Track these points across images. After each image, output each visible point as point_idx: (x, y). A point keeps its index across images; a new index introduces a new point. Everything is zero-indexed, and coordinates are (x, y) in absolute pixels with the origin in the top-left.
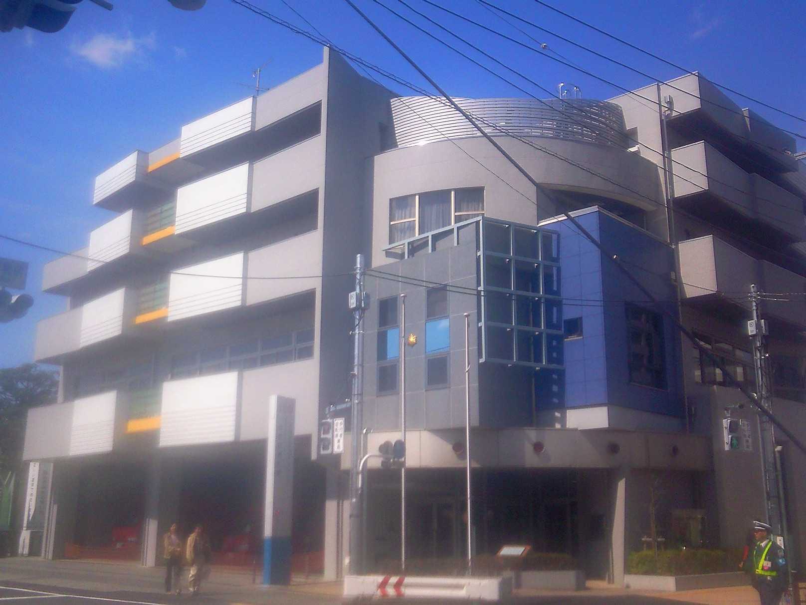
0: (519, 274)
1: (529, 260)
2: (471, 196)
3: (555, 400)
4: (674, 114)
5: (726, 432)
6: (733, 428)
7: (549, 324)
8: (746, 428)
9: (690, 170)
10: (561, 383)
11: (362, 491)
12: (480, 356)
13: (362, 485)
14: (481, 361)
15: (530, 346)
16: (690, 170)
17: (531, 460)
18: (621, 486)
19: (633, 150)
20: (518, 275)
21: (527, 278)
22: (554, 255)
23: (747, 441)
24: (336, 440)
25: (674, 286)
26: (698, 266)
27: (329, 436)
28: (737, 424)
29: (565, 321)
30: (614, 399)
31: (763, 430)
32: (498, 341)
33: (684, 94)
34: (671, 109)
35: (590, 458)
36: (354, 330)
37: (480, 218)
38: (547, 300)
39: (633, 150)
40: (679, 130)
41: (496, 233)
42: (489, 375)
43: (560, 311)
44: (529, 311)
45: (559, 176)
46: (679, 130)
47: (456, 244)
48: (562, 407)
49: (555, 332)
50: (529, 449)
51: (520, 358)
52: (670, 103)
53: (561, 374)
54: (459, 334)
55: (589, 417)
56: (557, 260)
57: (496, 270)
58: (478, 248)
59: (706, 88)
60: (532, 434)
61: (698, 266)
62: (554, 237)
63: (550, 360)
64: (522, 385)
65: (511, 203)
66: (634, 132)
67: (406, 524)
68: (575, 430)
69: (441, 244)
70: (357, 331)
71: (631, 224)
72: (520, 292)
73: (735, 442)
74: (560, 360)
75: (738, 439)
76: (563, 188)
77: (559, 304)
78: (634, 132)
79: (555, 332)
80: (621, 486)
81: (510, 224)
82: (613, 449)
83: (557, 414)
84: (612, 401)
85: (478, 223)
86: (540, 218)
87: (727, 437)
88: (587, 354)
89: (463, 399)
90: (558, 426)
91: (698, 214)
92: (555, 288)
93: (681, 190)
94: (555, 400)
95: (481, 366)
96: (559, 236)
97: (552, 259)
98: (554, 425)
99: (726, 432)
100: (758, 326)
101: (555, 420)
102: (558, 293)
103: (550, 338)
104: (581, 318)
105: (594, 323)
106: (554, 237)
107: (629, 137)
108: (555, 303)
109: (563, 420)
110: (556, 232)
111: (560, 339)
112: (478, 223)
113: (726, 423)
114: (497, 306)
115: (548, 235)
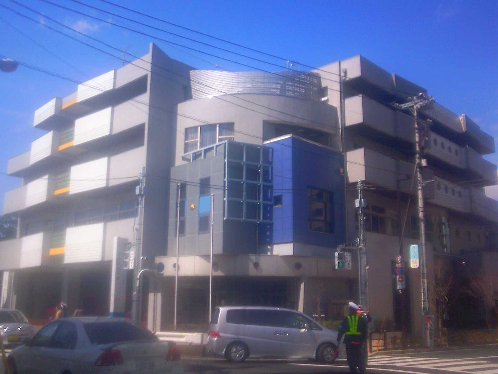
0: (248, 170)
1: (257, 164)
2: (228, 127)
3: (268, 240)
4: (347, 79)
5: (336, 259)
6: (340, 257)
7: (265, 198)
8: (348, 257)
9: (354, 111)
10: (271, 229)
11: (139, 288)
12: (224, 216)
13: (139, 284)
14: (225, 219)
15: (253, 210)
16: (354, 111)
17: (253, 272)
18: (302, 286)
19: (323, 99)
20: (248, 171)
21: (253, 173)
22: (270, 160)
23: (349, 264)
24: (130, 262)
25: (344, 176)
26: (356, 165)
27: (127, 260)
28: (343, 254)
29: (275, 197)
30: (296, 240)
31: (361, 258)
32: (233, 208)
33: (353, 68)
34: (345, 76)
35: (285, 271)
36: (138, 205)
37: (226, 141)
38: (264, 186)
39: (323, 99)
40: (350, 88)
41: (235, 149)
42: (230, 228)
43: (272, 192)
44: (253, 191)
45: (276, 117)
46: (350, 88)
47: (215, 155)
48: (271, 243)
49: (269, 203)
50: (251, 265)
51: (247, 217)
52: (345, 73)
53: (271, 225)
54: (214, 206)
55: (284, 249)
56: (271, 163)
57: (234, 169)
58: (225, 158)
59: (365, 64)
60: (253, 257)
61: (356, 165)
62: (271, 150)
63: (264, 218)
64: (247, 231)
65: (249, 133)
66: (326, 89)
67: (177, 303)
68: (277, 256)
69: (208, 154)
70: (139, 206)
71: (315, 144)
72: (248, 181)
73: (341, 264)
74: (271, 218)
75: (343, 263)
76: (277, 123)
77: (271, 187)
78: (326, 89)
79: (269, 203)
80: (302, 286)
81: (244, 144)
82: (298, 266)
83: (269, 247)
84: (295, 241)
85: (225, 143)
86: (265, 139)
87: (337, 262)
88: (283, 215)
89: (214, 240)
90: (269, 254)
91: (359, 135)
92: (270, 178)
93: (349, 122)
94: (268, 240)
95: (224, 221)
96: (273, 150)
97: (268, 162)
98: (267, 253)
99: (336, 259)
100: (360, 202)
101: (268, 250)
102: (271, 181)
103: (265, 206)
104: (281, 195)
105: (288, 200)
106: (271, 150)
107: (323, 91)
108: (268, 188)
109: (271, 250)
110: (271, 148)
111: (271, 206)
112: (225, 143)
113: (336, 254)
114: (234, 189)
115: (267, 150)
